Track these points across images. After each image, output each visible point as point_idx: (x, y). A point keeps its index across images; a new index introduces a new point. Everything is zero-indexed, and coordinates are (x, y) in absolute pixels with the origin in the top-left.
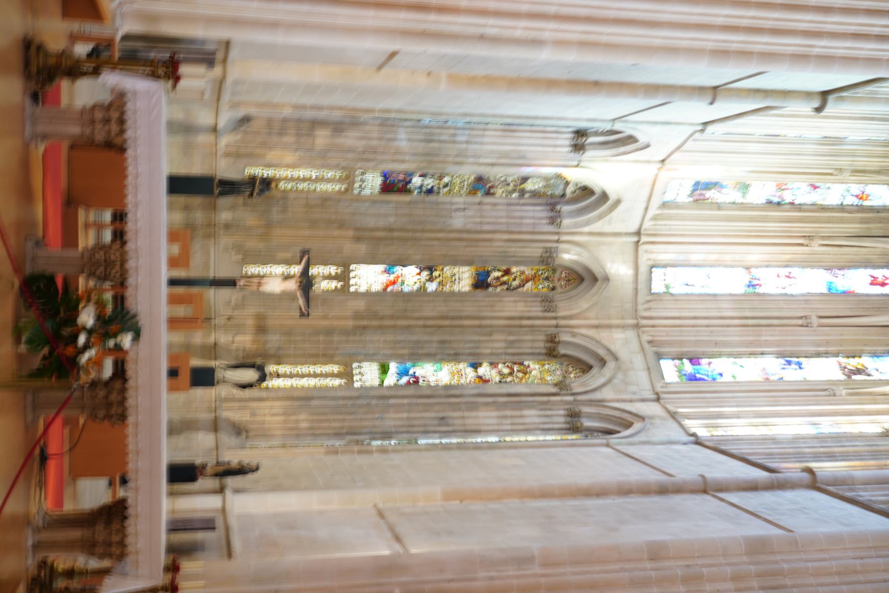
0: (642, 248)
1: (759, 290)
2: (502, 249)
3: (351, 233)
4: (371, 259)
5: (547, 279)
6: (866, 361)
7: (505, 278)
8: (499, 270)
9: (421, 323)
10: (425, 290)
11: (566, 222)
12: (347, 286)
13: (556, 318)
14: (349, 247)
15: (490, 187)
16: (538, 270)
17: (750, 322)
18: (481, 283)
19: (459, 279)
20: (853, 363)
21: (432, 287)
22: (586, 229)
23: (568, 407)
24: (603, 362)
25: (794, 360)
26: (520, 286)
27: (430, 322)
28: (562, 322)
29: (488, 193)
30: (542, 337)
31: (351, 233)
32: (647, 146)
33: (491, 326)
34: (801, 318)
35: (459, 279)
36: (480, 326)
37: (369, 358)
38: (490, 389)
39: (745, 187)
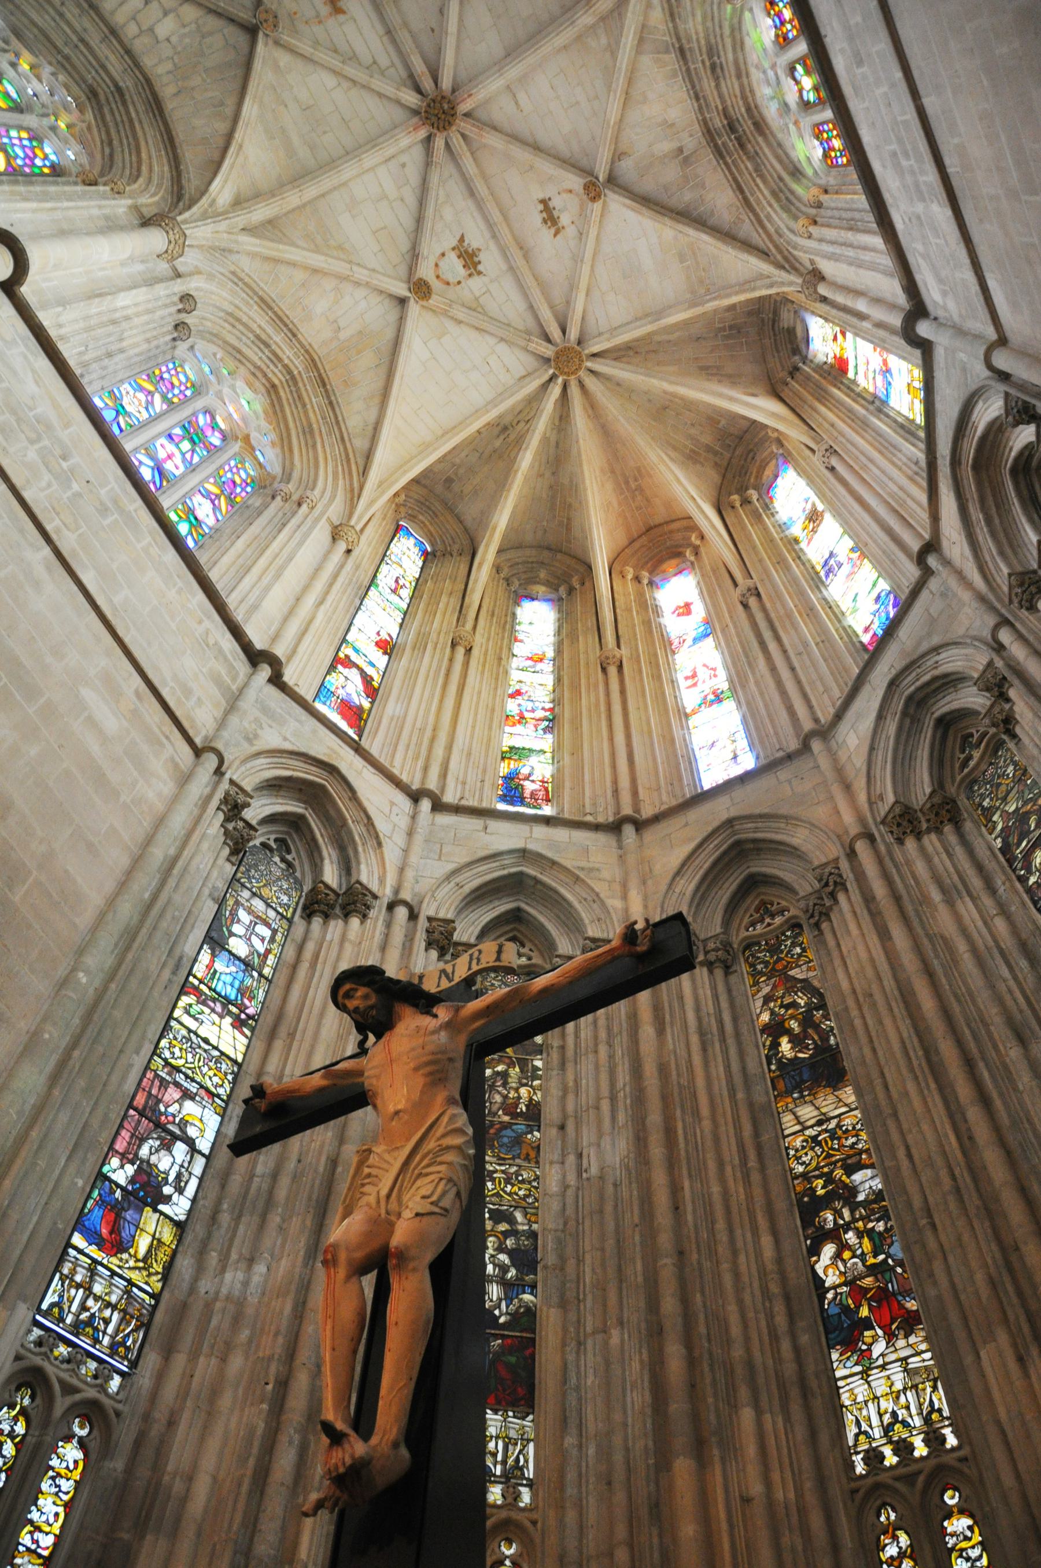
1: (725, 686)
2: (694, 1039)
3: (683, 1467)
5: (774, 950)
7: (794, 1025)
8: (775, 1045)
9: (974, 1114)
10: (879, 1196)
12: (941, 1471)
13: (851, 854)
15: (514, 1115)
16: (755, 974)
17: (767, 635)
19: (820, 1123)
23: (1024, 613)
25: (822, 574)
26: (806, 986)
27: (964, 1091)
30: (910, 843)
31: (683, 1467)
32: (331, 769)
33: (917, 948)
34: (745, 606)
35: (820, 1123)
36: (930, 974)
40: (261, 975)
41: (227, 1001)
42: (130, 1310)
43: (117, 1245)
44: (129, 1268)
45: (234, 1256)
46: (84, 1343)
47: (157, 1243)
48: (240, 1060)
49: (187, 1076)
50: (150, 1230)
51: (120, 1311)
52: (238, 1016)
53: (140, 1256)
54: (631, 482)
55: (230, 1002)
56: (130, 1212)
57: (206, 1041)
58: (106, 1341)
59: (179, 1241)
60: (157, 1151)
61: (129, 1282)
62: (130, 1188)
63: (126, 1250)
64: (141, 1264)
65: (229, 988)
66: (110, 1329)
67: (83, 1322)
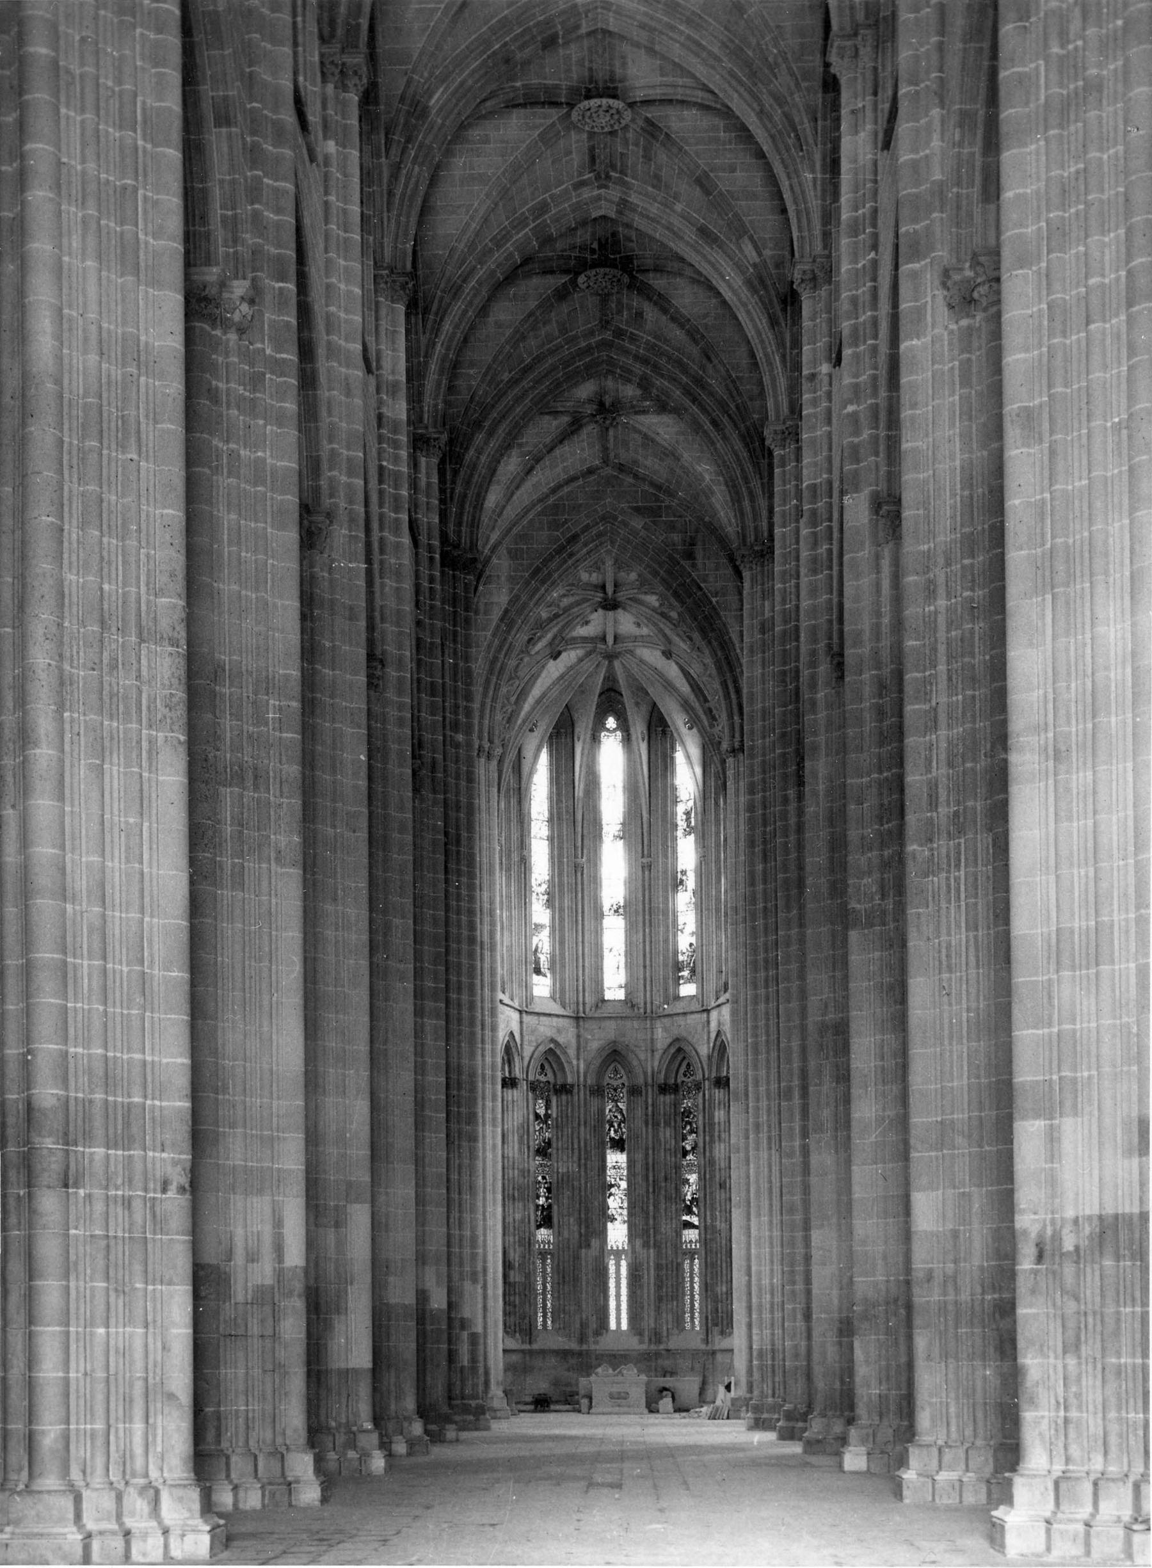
0: (589, 1013)
4: (603, 1233)
6: (681, 809)
11: (570, 1080)
14: (594, 1252)
18: (619, 1145)
20: (681, 824)
21: (624, 1185)
22: (575, 1062)
24: (679, 1050)
26: (621, 1112)
28: (650, 1080)
29: (549, 1144)
37: (679, 1235)
38: (701, 1144)
39: (539, 927)
54: (610, 678)
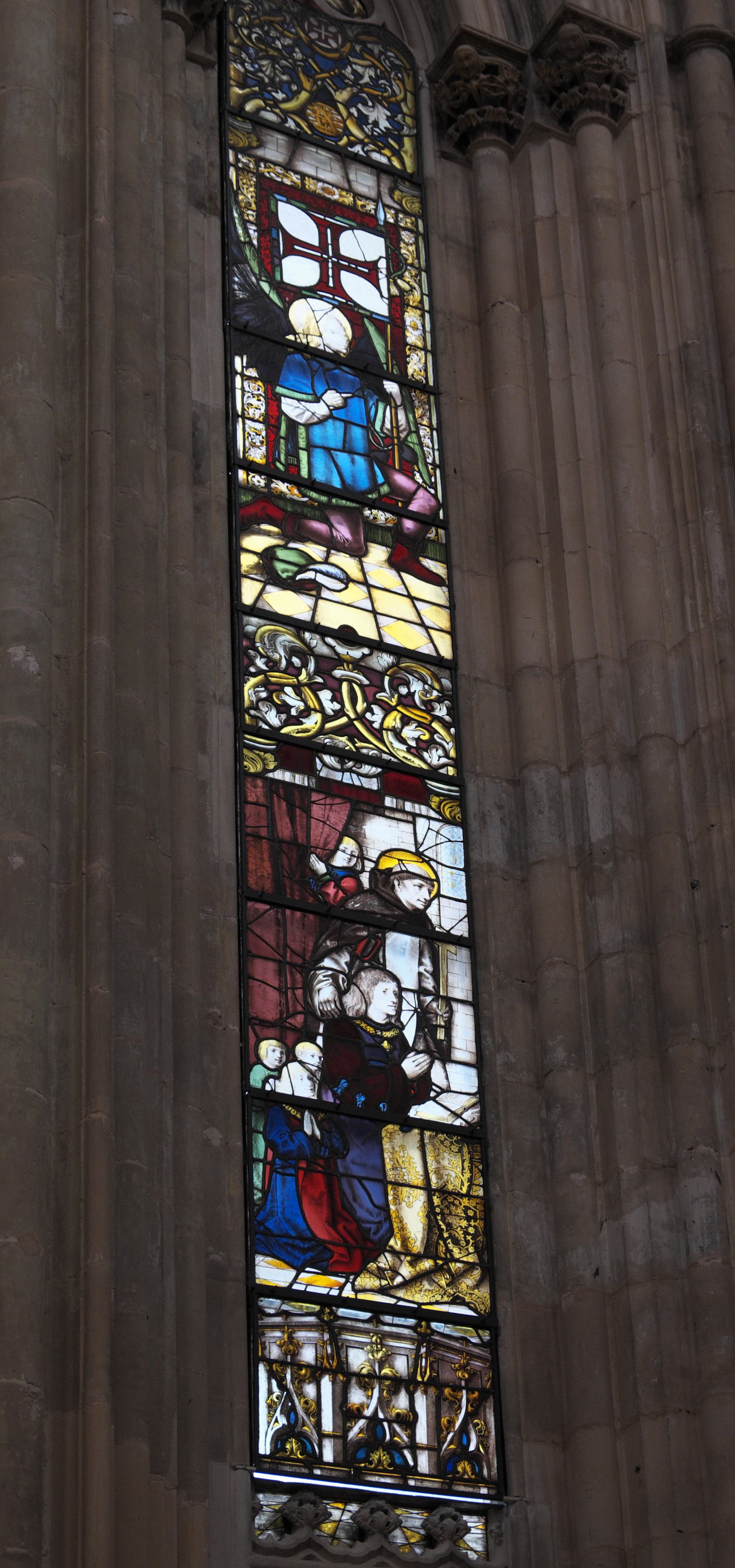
40: (407, 384)
41: (352, 501)
42: (446, 1375)
43: (358, 1241)
44: (406, 1284)
45: (629, 1170)
46: (382, 1485)
47: (439, 1198)
48: (445, 650)
49: (342, 755)
50: (415, 1181)
51: (426, 1385)
52: (397, 528)
53: (417, 1246)
55: (362, 500)
56: (353, 1155)
57: (347, 635)
58: (424, 1462)
59: (484, 1174)
60: (352, 979)
61: (420, 1314)
62: (329, 1098)
63: (382, 1247)
64: (427, 1264)
65: (343, 459)
66: (422, 1435)
67: (359, 1444)
